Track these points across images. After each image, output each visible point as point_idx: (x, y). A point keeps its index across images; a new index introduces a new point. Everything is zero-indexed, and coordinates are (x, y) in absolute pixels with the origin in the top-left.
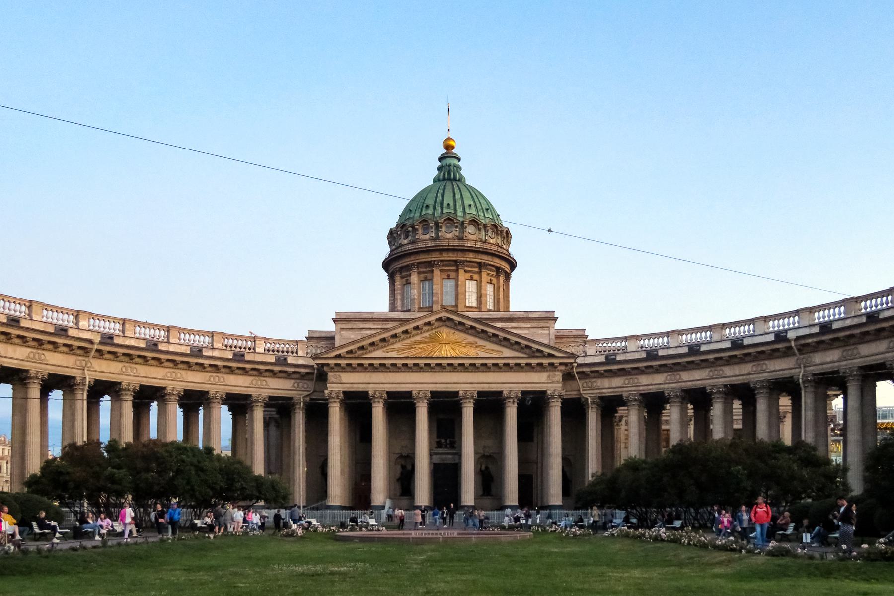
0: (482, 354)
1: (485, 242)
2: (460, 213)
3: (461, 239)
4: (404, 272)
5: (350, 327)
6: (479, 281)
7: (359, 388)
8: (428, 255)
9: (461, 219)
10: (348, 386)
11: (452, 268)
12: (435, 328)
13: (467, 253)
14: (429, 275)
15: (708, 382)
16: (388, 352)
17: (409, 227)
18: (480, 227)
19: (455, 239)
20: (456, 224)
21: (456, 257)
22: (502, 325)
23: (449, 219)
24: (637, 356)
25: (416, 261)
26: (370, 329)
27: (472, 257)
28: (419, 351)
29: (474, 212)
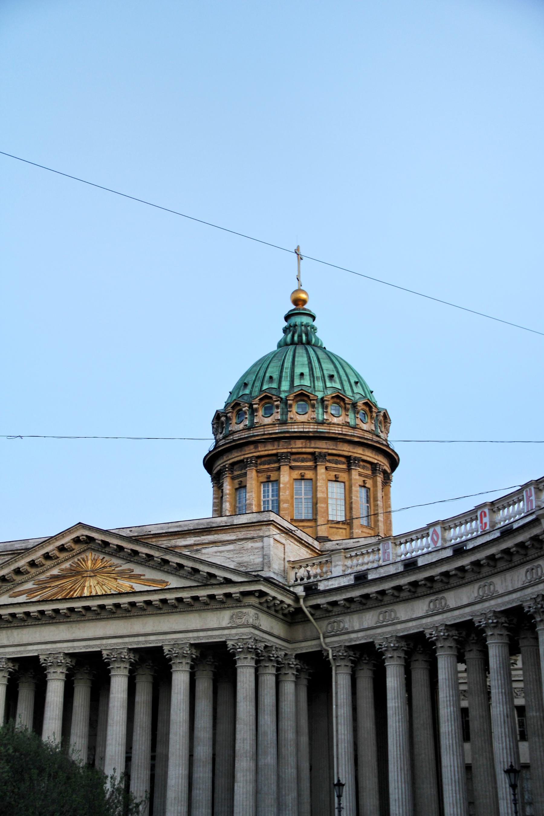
0: (138, 587)
1: (322, 423)
2: (285, 386)
3: (284, 422)
6: (314, 480)
8: (241, 451)
9: (283, 395)
11: (273, 466)
12: (78, 554)
13: (292, 442)
15: (477, 607)
16: (15, 597)
18: (312, 402)
19: (275, 424)
22: (195, 541)
24: (392, 570)
25: (229, 462)
27: (301, 446)
28: (55, 590)
29: (307, 382)
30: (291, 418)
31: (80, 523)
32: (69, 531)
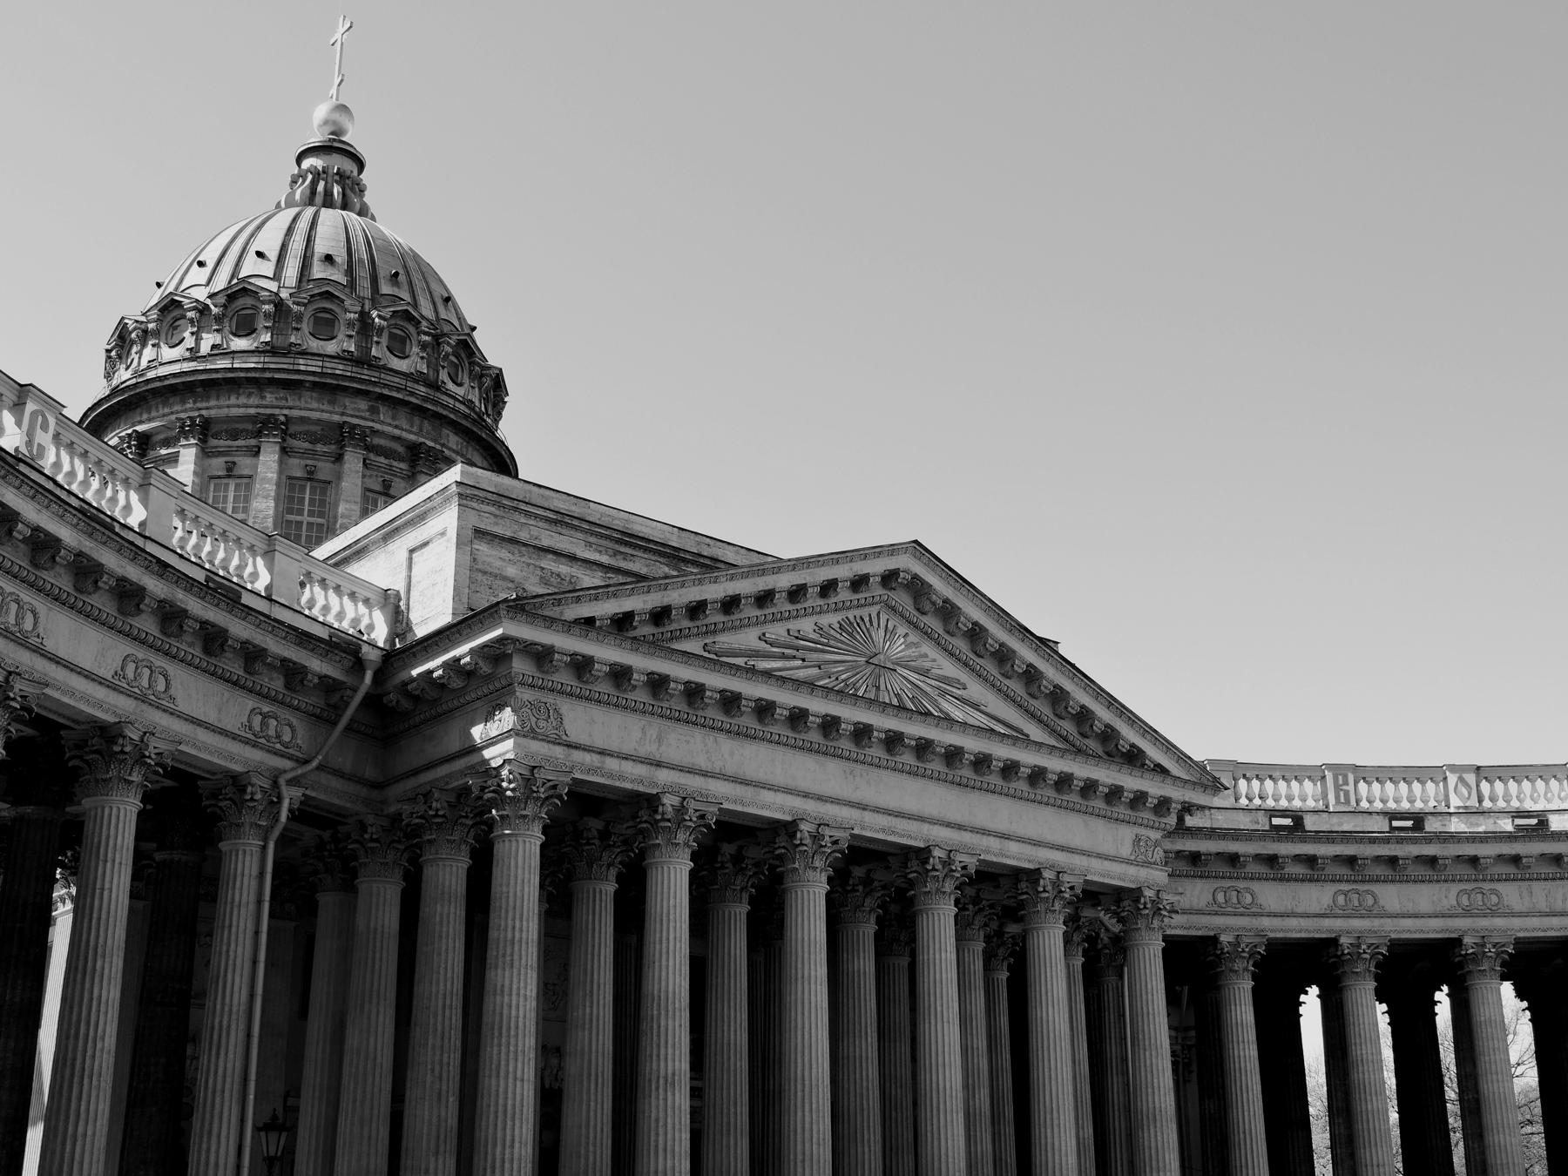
2: (426, 310)
4: (215, 436)
5: (509, 534)
7: (621, 777)
8: (332, 402)
10: (588, 758)
11: (395, 464)
14: (325, 469)
17: (269, 302)
20: (427, 338)
21: (415, 434)
23: (407, 316)
24: (1243, 822)
25: (286, 412)
26: (572, 558)
27: (454, 447)
30: (443, 382)
31: (916, 542)
32: (892, 550)
